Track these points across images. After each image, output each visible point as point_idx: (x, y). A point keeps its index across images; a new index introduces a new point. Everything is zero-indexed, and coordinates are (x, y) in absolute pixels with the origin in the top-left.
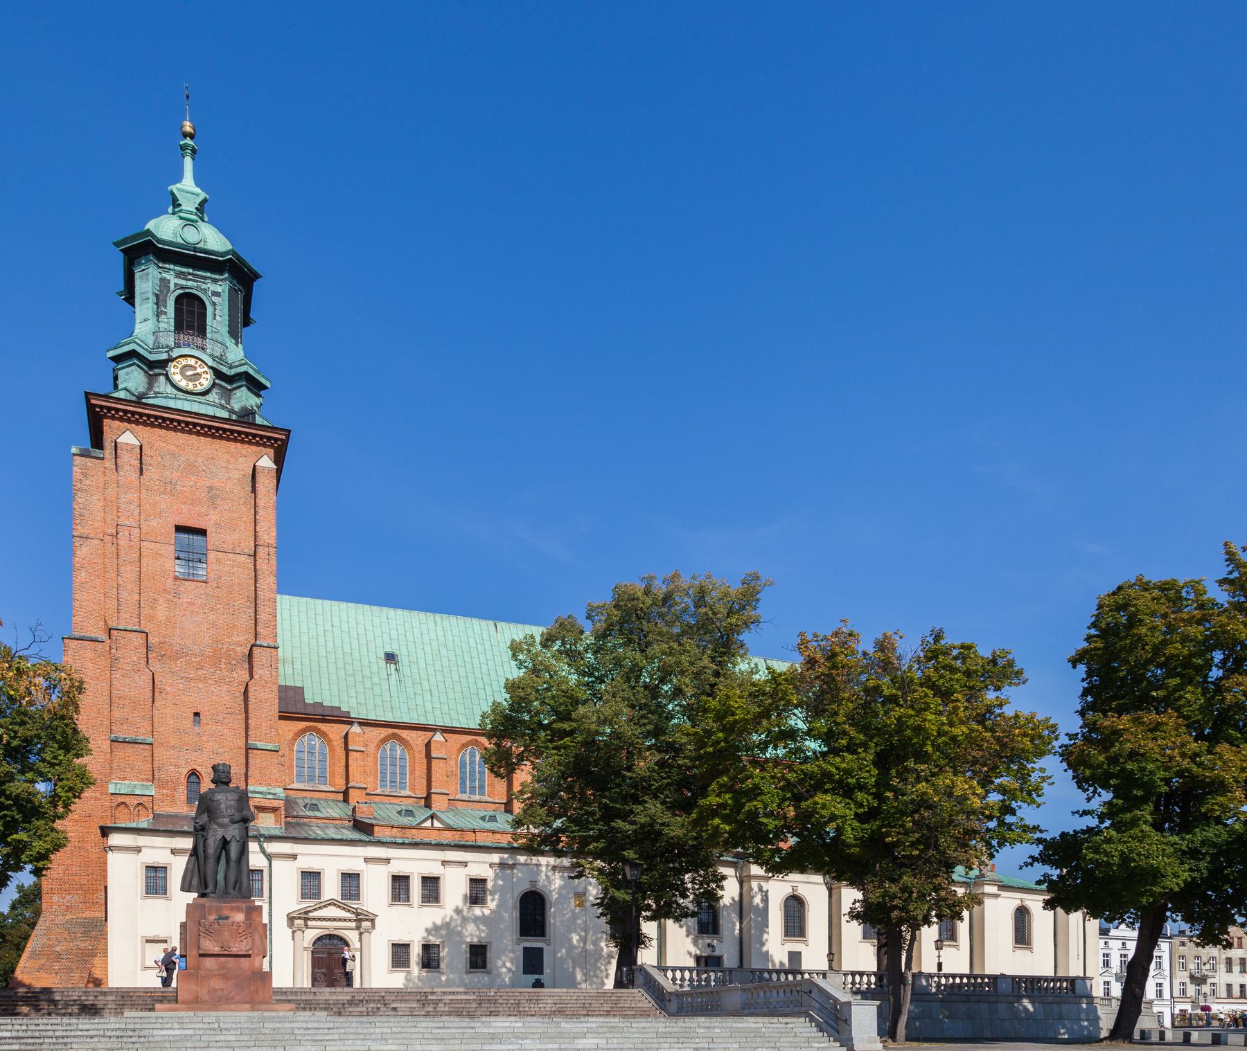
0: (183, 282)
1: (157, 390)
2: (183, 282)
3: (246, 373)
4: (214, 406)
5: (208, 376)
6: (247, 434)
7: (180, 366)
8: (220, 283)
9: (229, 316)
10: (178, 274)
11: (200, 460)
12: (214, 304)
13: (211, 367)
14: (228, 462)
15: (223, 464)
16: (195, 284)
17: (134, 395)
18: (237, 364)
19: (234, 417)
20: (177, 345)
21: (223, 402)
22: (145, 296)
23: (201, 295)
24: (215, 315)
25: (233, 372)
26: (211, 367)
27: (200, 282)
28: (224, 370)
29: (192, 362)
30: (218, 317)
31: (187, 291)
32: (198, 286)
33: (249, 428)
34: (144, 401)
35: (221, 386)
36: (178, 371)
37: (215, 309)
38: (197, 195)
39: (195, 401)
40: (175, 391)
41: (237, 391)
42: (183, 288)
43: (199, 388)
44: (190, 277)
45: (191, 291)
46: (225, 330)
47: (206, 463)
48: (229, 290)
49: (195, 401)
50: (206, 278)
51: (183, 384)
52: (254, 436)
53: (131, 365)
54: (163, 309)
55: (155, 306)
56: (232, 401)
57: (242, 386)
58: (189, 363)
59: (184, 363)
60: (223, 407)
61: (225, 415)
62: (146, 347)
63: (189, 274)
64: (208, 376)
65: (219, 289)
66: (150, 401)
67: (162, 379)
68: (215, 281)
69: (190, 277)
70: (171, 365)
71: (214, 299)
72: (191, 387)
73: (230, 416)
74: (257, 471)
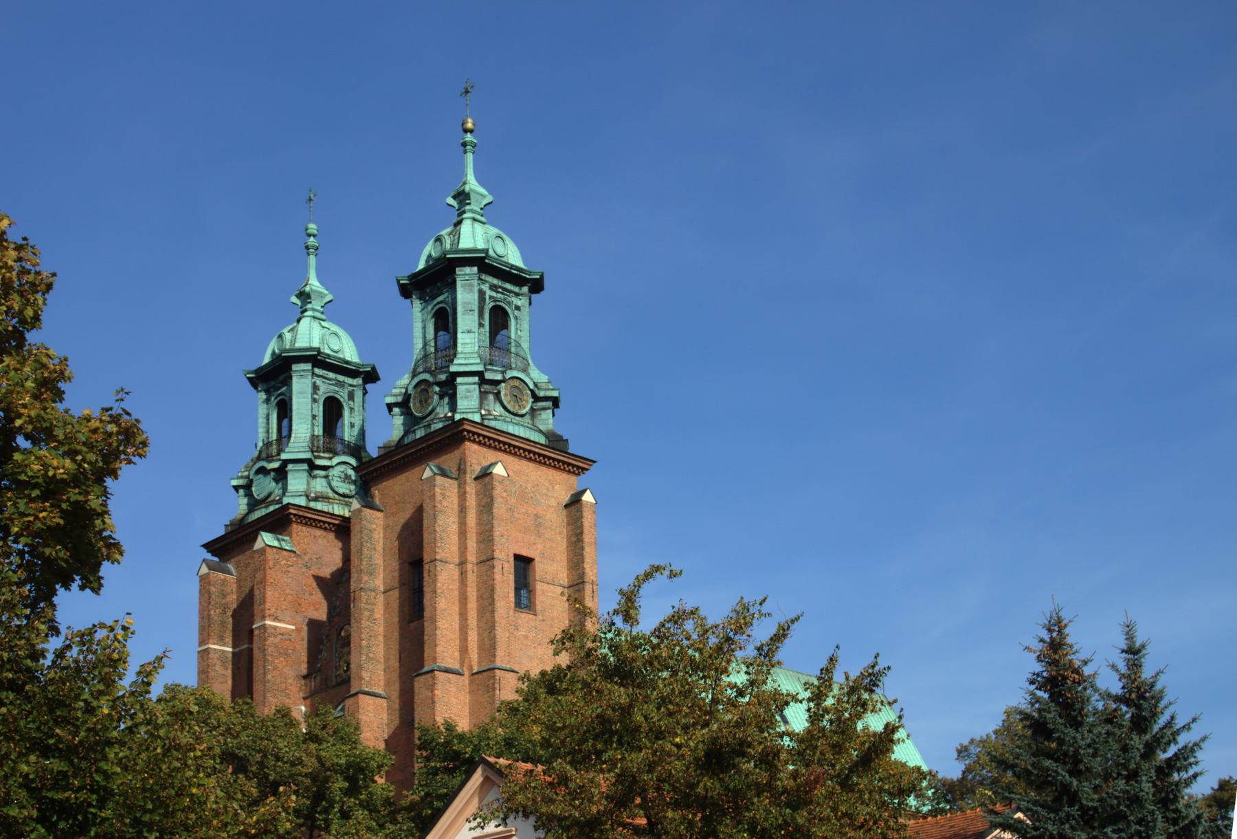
10: (493, 288)
11: (529, 486)
15: (545, 491)
16: (502, 296)
22: (469, 307)
29: (517, 383)
31: (498, 303)
32: (505, 299)
38: (484, 196)
41: (542, 412)
42: (496, 300)
44: (500, 290)
50: (510, 292)
65: (519, 303)
67: (491, 397)
69: (500, 290)
71: (516, 312)
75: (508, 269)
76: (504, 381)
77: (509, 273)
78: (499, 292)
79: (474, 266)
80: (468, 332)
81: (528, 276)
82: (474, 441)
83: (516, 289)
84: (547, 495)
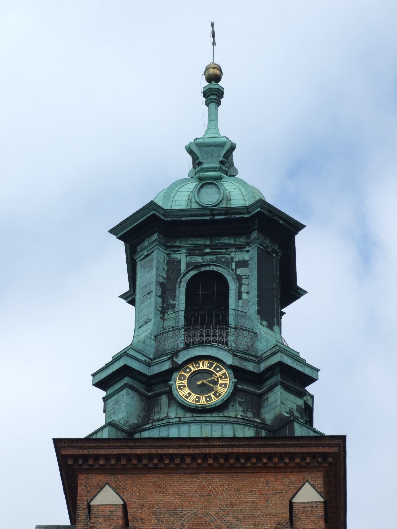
0: (199, 259)
1: (157, 417)
2: (199, 259)
3: (280, 364)
4: (234, 423)
5: (227, 381)
6: (281, 456)
7: (187, 375)
8: (247, 249)
9: (259, 289)
12: (239, 278)
13: (231, 367)
14: (255, 506)
16: (214, 257)
17: (122, 430)
18: (268, 353)
19: (263, 434)
20: (187, 346)
21: (250, 415)
23: (220, 270)
24: (240, 294)
25: (263, 366)
26: (231, 367)
27: (221, 253)
28: (250, 367)
29: (204, 365)
30: (244, 296)
31: (203, 269)
32: (218, 260)
33: (284, 445)
34: (137, 436)
35: (247, 392)
36: (185, 382)
37: (240, 285)
39: (206, 421)
40: (181, 413)
42: (197, 266)
43: (215, 400)
44: (208, 250)
45: (208, 268)
46: (253, 310)
47: (221, 513)
48: (259, 255)
49: (206, 421)
50: (227, 247)
51: (192, 399)
52: (292, 456)
53: (122, 388)
54: (171, 302)
55: (160, 300)
56: (263, 411)
57: (275, 385)
58: (201, 367)
59: (193, 369)
60: (246, 422)
61: (249, 432)
62: (143, 358)
63: (206, 246)
64: (227, 381)
65: (245, 256)
66: (146, 435)
67: (164, 399)
68: (240, 248)
70: (176, 375)
72: (203, 401)
73: (257, 433)
74: (296, 511)
75: (208, 218)
76: (176, 368)
77: (213, 222)
78: (208, 254)
79: (153, 234)
80: (146, 323)
81: (246, 216)
82: (91, 470)
83: (242, 240)
84: (253, 516)
